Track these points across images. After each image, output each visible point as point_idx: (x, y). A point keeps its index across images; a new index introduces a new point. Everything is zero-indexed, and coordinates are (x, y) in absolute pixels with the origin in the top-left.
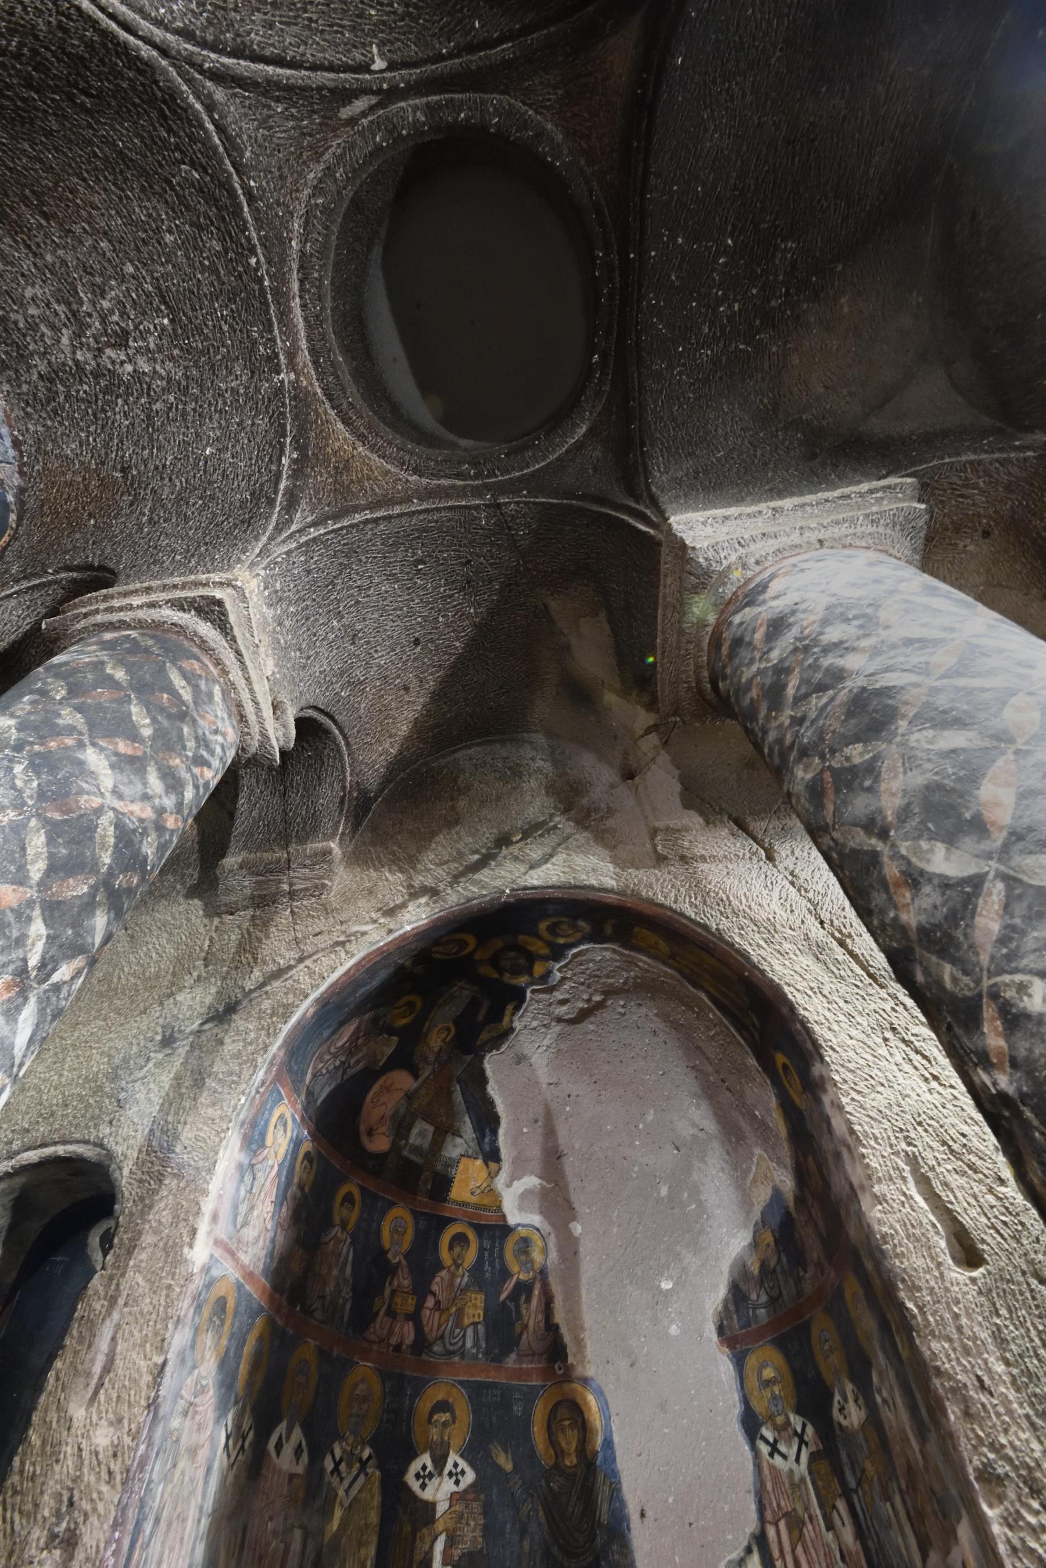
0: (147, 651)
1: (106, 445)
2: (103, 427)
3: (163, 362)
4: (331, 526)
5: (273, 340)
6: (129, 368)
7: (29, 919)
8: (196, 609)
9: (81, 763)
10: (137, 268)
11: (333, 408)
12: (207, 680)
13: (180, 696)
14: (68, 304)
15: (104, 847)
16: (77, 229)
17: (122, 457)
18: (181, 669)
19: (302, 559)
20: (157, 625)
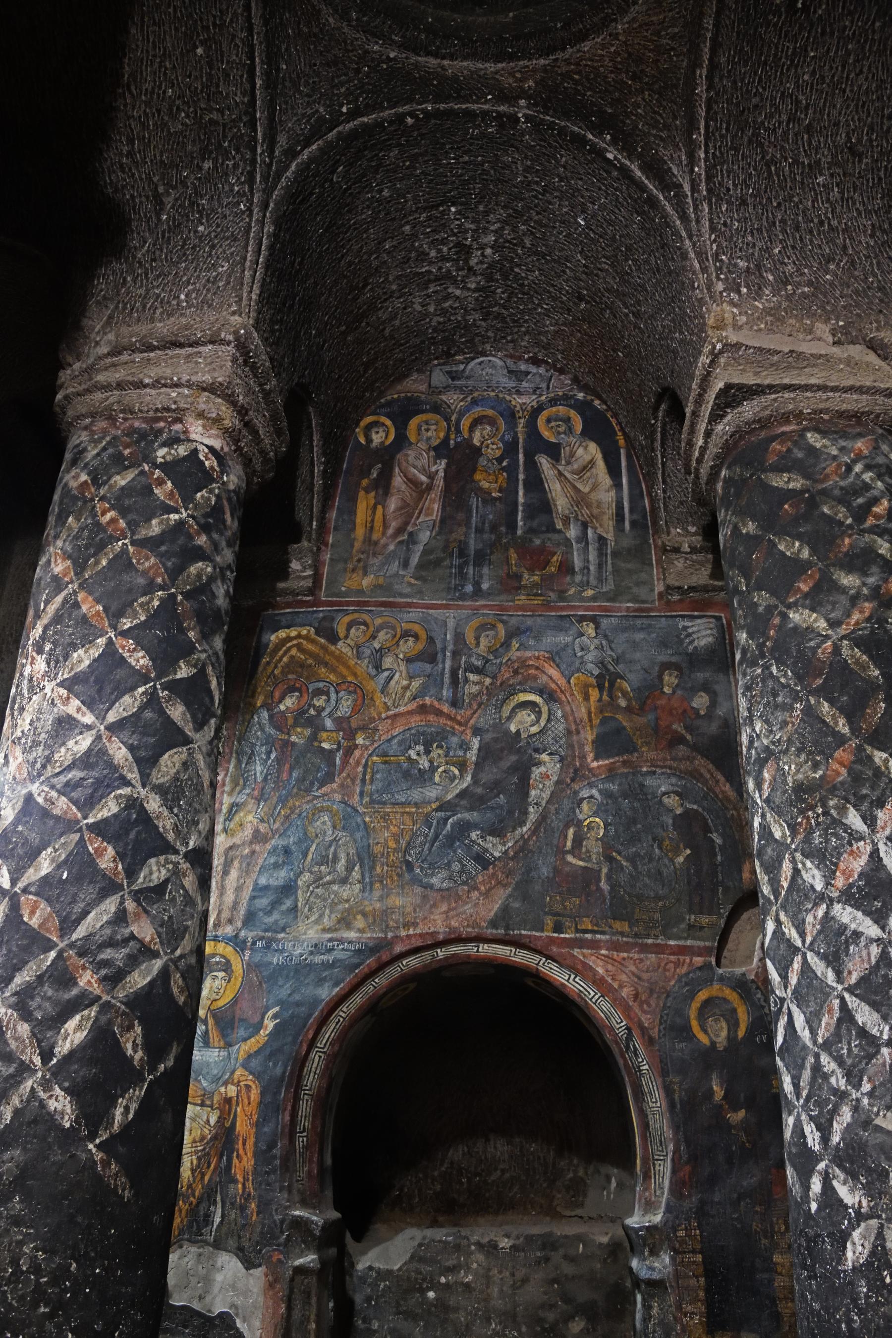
1: (555, 299)
2: (536, 292)
3: (488, 222)
4: (699, 137)
5: (485, 114)
6: (489, 251)
7: (870, 758)
9: (796, 628)
10: (407, 223)
11: (564, 49)
13: (793, 490)
15: (865, 668)
16: (375, 263)
17: (567, 292)
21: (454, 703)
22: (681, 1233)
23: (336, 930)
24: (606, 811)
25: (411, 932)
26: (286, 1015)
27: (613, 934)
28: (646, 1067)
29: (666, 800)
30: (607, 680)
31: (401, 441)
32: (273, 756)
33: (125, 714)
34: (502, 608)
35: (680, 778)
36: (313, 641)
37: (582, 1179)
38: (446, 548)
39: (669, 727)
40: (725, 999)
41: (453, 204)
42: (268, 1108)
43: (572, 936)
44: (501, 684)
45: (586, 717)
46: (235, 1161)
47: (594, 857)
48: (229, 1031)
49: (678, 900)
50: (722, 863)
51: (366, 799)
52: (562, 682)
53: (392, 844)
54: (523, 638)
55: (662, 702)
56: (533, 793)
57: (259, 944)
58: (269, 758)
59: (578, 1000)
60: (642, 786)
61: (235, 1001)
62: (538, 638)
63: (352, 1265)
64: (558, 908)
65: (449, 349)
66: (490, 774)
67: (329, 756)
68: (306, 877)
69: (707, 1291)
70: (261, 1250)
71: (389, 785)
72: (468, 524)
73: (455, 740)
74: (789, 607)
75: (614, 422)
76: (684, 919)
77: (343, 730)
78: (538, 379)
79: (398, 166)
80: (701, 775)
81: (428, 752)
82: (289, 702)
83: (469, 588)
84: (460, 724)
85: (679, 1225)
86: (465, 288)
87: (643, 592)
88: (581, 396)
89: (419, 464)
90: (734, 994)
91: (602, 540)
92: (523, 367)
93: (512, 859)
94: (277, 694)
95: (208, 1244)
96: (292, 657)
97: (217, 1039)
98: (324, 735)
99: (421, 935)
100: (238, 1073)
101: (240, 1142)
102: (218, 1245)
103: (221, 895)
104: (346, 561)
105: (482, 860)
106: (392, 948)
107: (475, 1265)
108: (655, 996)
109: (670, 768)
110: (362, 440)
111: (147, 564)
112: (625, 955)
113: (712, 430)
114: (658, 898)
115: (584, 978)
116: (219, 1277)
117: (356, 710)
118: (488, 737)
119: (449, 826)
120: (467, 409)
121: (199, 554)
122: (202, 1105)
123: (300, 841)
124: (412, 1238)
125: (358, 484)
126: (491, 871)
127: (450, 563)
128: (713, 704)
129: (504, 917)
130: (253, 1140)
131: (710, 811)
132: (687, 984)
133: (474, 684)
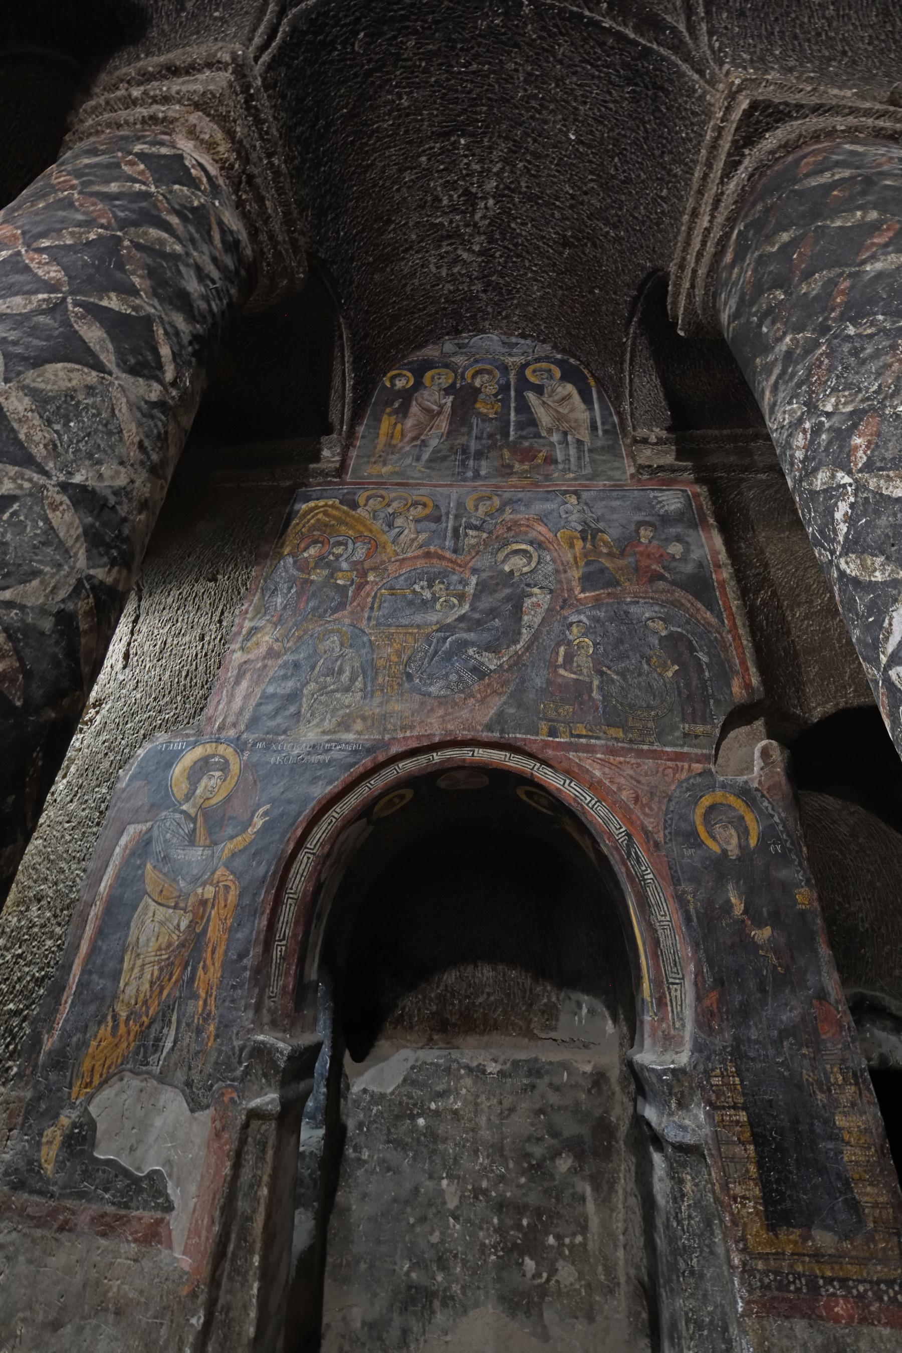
0: (767, 211)
1: (542, 255)
2: (528, 252)
8: (745, 146)
9: (880, 275)
12: (833, 153)
14: (442, 238)
16: (397, 197)
17: (555, 242)
18: (807, 176)
19: (725, 15)
20: (742, 199)
21: (455, 551)
22: (716, 1081)
23: (335, 732)
24: (595, 633)
25: (408, 734)
26: (276, 812)
27: (608, 739)
28: (651, 876)
29: (649, 623)
30: (589, 533)
31: (418, 385)
32: (293, 591)
33: (9, 311)
34: (496, 486)
35: (662, 606)
36: (337, 509)
37: (555, 1004)
38: (452, 448)
39: (649, 566)
40: (730, 806)
41: (463, 136)
42: (244, 912)
43: (567, 740)
44: (497, 537)
45: (572, 560)
46: (200, 972)
47: (585, 671)
48: (217, 829)
49: (670, 710)
50: (710, 679)
51: (373, 622)
52: (550, 535)
53: (394, 658)
54: (516, 506)
55: (641, 549)
56: (526, 618)
57: (259, 745)
58: (289, 592)
59: (575, 805)
60: (627, 613)
61: (228, 799)
62: (527, 505)
63: (348, 1087)
64: (552, 714)
65: (457, 325)
66: (485, 603)
67: (343, 590)
68: (312, 686)
69: (760, 1165)
70: (212, 1085)
71: (395, 610)
72: (469, 433)
73: (455, 578)
74: (864, 262)
75: (586, 372)
76: (678, 728)
77: (357, 570)
78: (525, 348)
79: (414, 65)
80: (682, 605)
81: (430, 586)
82: (312, 551)
83: (470, 474)
84: (460, 566)
85: (713, 1070)
86: (470, 250)
87: (617, 474)
88: (559, 356)
89: (432, 399)
90: (739, 801)
91: (579, 443)
92: (514, 340)
93: (507, 671)
94: (302, 546)
95: (153, 1077)
96: (318, 520)
97: (203, 838)
98: (340, 574)
99: (418, 738)
100: (218, 873)
101: (210, 949)
102: (163, 1079)
103: (230, 702)
104: (369, 457)
105: (478, 672)
106: (389, 749)
107: (464, 1091)
108: (656, 799)
109: (652, 598)
110: (388, 384)
111: (92, 208)
112: (622, 759)
113: (722, 193)
114: (650, 708)
115: (580, 782)
116: (158, 1122)
117: (369, 556)
118: (484, 575)
119: (447, 644)
120: (471, 366)
121: (166, 227)
122: (176, 907)
123: (310, 656)
124: (406, 1060)
125: (383, 411)
126: (487, 681)
127: (456, 457)
128: (687, 550)
129: (500, 719)
130: (223, 947)
131: (693, 634)
132: (688, 790)
133: (472, 538)
